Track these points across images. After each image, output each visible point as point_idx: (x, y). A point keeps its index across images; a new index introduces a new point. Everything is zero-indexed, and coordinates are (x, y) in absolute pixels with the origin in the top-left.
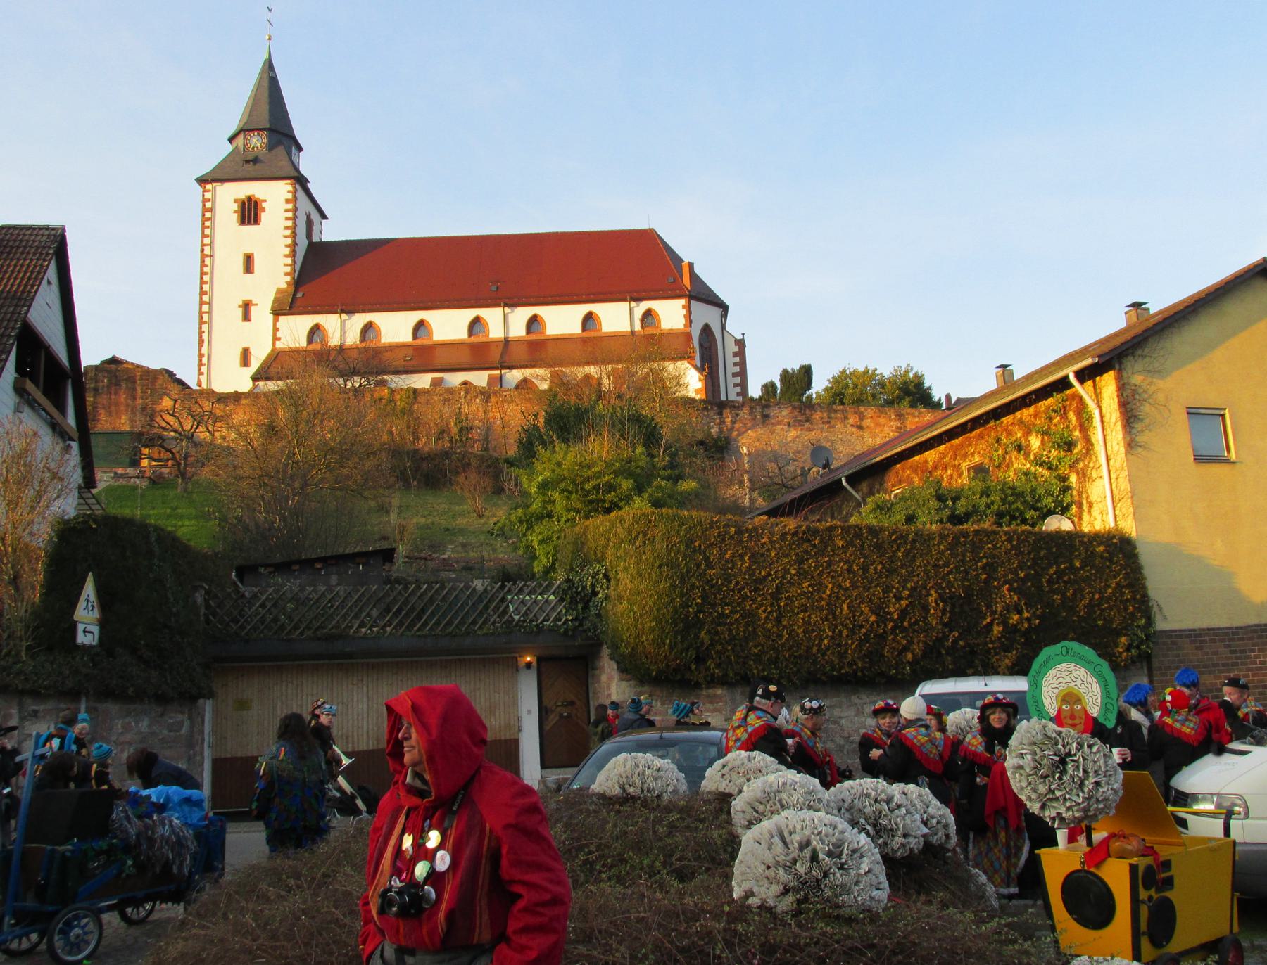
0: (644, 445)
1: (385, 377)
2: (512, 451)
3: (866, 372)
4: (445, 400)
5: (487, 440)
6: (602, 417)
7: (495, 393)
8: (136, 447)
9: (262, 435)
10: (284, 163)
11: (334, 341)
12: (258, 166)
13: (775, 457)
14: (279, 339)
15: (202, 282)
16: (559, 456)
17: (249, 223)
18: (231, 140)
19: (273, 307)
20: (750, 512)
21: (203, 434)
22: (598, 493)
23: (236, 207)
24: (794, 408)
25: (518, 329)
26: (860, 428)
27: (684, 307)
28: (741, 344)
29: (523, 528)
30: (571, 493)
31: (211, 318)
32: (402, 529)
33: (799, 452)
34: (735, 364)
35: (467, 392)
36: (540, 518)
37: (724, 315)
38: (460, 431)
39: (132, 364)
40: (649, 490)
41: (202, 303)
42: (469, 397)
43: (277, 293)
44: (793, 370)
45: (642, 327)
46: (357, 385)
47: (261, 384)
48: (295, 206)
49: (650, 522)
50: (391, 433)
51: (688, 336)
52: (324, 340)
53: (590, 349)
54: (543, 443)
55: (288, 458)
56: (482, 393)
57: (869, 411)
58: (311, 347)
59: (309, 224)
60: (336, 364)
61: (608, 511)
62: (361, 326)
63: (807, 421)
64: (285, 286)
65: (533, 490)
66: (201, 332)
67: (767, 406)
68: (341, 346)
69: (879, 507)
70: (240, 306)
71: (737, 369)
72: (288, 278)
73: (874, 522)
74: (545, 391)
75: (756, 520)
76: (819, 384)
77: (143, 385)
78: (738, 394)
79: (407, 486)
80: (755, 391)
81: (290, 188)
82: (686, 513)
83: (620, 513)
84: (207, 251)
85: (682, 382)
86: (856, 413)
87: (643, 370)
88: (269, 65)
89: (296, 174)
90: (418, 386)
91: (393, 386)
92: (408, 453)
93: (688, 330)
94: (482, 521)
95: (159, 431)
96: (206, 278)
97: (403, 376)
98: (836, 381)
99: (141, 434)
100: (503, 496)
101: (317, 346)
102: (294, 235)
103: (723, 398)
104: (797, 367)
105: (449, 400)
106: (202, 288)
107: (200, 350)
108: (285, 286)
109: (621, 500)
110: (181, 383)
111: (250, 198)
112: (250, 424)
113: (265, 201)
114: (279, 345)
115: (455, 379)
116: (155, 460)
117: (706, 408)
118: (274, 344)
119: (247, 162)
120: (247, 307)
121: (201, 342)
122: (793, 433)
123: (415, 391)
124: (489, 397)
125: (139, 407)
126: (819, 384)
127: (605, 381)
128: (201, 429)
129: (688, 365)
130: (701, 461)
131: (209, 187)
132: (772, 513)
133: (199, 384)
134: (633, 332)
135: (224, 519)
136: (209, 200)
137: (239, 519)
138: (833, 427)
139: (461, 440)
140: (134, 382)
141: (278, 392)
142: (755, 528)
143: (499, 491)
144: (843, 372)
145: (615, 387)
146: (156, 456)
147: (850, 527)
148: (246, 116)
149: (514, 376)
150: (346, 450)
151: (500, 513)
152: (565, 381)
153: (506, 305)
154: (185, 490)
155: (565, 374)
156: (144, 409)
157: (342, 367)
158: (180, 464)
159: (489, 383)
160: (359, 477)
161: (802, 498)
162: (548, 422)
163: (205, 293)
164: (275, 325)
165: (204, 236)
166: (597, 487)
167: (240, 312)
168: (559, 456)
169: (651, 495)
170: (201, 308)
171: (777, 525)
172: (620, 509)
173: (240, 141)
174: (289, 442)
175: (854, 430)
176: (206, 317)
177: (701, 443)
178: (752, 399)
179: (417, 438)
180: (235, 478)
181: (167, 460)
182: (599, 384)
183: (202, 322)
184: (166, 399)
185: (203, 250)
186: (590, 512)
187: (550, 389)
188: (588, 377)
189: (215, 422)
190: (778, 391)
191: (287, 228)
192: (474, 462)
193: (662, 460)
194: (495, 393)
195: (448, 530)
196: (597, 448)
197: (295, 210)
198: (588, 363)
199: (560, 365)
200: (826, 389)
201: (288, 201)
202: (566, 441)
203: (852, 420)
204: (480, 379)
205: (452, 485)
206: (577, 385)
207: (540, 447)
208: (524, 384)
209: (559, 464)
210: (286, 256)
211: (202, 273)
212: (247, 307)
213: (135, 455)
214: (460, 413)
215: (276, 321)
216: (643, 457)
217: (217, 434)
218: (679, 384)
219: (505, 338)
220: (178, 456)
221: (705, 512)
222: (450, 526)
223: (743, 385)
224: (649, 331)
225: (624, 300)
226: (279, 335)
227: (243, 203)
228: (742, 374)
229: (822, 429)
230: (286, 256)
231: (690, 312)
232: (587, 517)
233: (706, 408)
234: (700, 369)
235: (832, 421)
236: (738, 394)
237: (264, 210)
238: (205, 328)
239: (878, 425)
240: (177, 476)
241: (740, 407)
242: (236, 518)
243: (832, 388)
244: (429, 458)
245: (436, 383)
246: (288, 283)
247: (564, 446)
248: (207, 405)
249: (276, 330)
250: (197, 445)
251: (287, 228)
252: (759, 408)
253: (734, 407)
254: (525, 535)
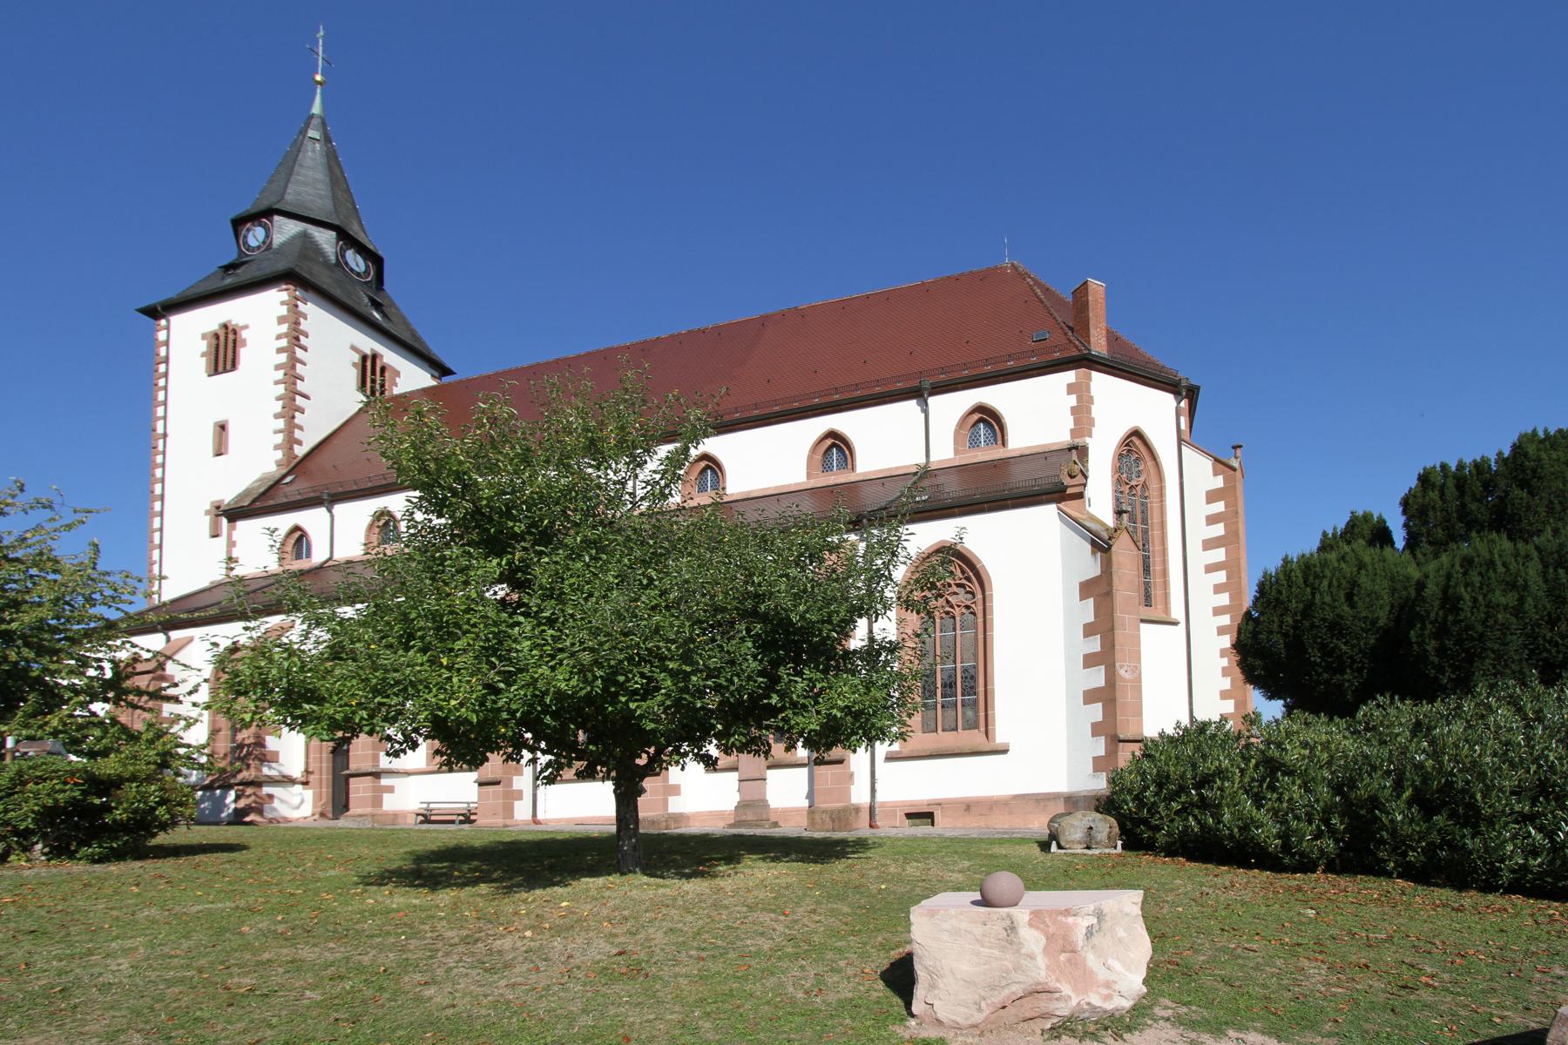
17: (225, 371)
23: (203, 346)
111: (225, 326)
113: (246, 327)
191: (278, 367)
201: (281, 320)
210: (277, 416)
227: (217, 336)
230: (277, 416)
237: (244, 343)
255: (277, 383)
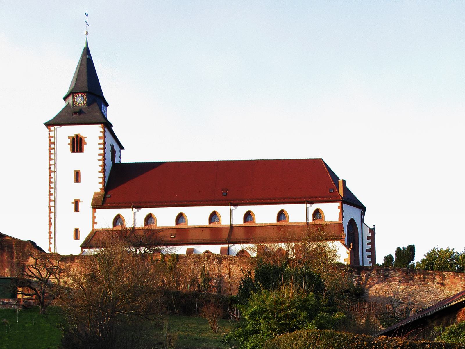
0: (314, 292)
1: (160, 247)
2: (235, 293)
3: (448, 251)
4: (195, 262)
5: (220, 287)
6: (289, 274)
7: (225, 258)
8: (15, 287)
9: (88, 281)
10: (98, 114)
11: (129, 225)
12: (82, 116)
13: (391, 300)
14: (96, 223)
15: (50, 188)
16: (264, 297)
17: (77, 151)
18: (65, 99)
19: (92, 203)
20: (375, 334)
21: (53, 280)
22: (286, 319)
23: (69, 141)
24: (403, 271)
25: (239, 220)
26: (443, 284)
27: (339, 208)
28: (372, 231)
29: (242, 339)
30: (270, 319)
31: (55, 209)
32: (170, 338)
33: (405, 298)
34: (369, 244)
35: (208, 257)
36: (251, 334)
37: (363, 214)
38: (204, 281)
39: (11, 237)
40: (316, 318)
41: (50, 200)
42: (209, 261)
43: (94, 195)
44: (403, 248)
45: (313, 220)
46: (143, 252)
47: (86, 250)
48: (104, 141)
49: (317, 337)
50: (163, 281)
51: (341, 226)
52: (123, 224)
53: (282, 232)
54: (254, 289)
55: (104, 295)
56: (217, 258)
57: (448, 275)
58: (115, 229)
59: (113, 152)
60: (131, 239)
61: (292, 330)
62: (145, 216)
63: (411, 280)
64: (99, 191)
65: (247, 317)
66: (50, 218)
67: (387, 270)
68: (133, 228)
69: (452, 332)
70: (72, 203)
71: (370, 247)
72: (101, 186)
73: (449, 341)
74: (255, 257)
75: (380, 338)
76: (419, 257)
77: (17, 250)
78: (370, 262)
79: (173, 313)
80: (380, 261)
81: (101, 130)
82: (338, 333)
83: (300, 331)
84: (53, 169)
85: (337, 254)
86: (440, 275)
87: (314, 246)
88: (87, 51)
89: (105, 121)
90: (178, 253)
91: (164, 253)
92: (174, 293)
93: (341, 222)
94: (217, 335)
95: (26, 277)
96: (52, 185)
97: (170, 247)
98: (429, 255)
99: (17, 279)
100: (230, 320)
101: (119, 228)
102: (104, 159)
103: (361, 264)
104: (406, 247)
105: (198, 262)
106: (50, 191)
107: (50, 229)
108: (99, 191)
109: (300, 324)
110: (39, 249)
111: (77, 136)
112: (81, 275)
113: (86, 138)
114: (97, 227)
115: (201, 249)
116: (26, 295)
117: (350, 270)
118: (93, 226)
119: (75, 113)
120: (76, 203)
121: (50, 224)
122: (402, 287)
123: (177, 256)
124: (221, 261)
125: (15, 263)
126: (419, 257)
127: (291, 252)
128: (52, 277)
129: (341, 244)
130: (346, 302)
131: (52, 128)
132: (388, 334)
133: (50, 250)
134: (307, 223)
135: (67, 330)
136: (53, 137)
137: (76, 331)
138: (427, 284)
139: (205, 286)
140: (12, 248)
141: (97, 255)
142: (379, 343)
143: (227, 317)
144: (434, 250)
145: (296, 256)
146: (26, 292)
147: (435, 344)
148: (74, 83)
149: (236, 248)
150: (138, 291)
151: (228, 331)
152: (267, 251)
153: (231, 204)
154: (44, 313)
155: (266, 247)
156: (18, 264)
157: (134, 241)
158: (40, 297)
159: (221, 252)
160: (145, 307)
161: (407, 325)
162: (256, 276)
163: (52, 195)
164: (93, 215)
165: (50, 159)
166: (285, 316)
167: (73, 206)
168: (264, 297)
169: (317, 322)
170: (49, 204)
171: (392, 341)
172: (299, 329)
173: (70, 99)
174: (104, 286)
175: (439, 286)
176: (52, 209)
177: (347, 291)
178: (378, 265)
179: (179, 285)
180: (73, 306)
181: (32, 295)
182: (287, 253)
183: (50, 212)
184: (31, 258)
185: (50, 168)
186: (281, 330)
187: (258, 256)
188: (280, 250)
189: (60, 273)
190: (394, 261)
191: (100, 155)
192: (212, 300)
193: (324, 301)
194: (225, 258)
195: (197, 339)
196: (286, 293)
197: (105, 143)
198: (281, 241)
199: (264, 242)
200: (423, 260)
201: (100, 138)
202: (267, 288)
203: (438, 279)
204: (216, 249)
205: (199, 313)
206: (274, 254)
207: (252, 292)
208: (242, 253)
209: (263, 302)
210: (100, 172)
211: (50, 182)
212: (76, 203)
213: (14, 291)
214: (204, 270)
215: (94, 212)
216: (313, 298)
217: (61, 280)
218: (335, 255)
219: (231, 225)
220: (39, 292)
221: (350, 332)
222: (198, 338)
223: (373, 256)
224: (318, 222)
225: (303, 203)
226: (96, 221)
227: (73, 139)
228: (373, 250)
229: (419, 285)
230: (100, 172)
231: (342, 211)
232: (280, 333)
233: (350, 270)
234: (348, 247)
235: (426, 280)
236: (370, 262)
237: (86, 143)
238: (52, 215)
239: (453, 283)
240: (39, 304)
241: (371, 270)
242: (74, 330)
243: (426, 260)
244: (186, 296)
245: (190, 251)
246: (101, 189)
247: (267, 291)
248: (55, 263)
249: (94, 218)
250: (51, 286)
251: (100, 155)
252: (382, 271)
253: (368, 270)
254: (243, 343)
255: (99, 160)
